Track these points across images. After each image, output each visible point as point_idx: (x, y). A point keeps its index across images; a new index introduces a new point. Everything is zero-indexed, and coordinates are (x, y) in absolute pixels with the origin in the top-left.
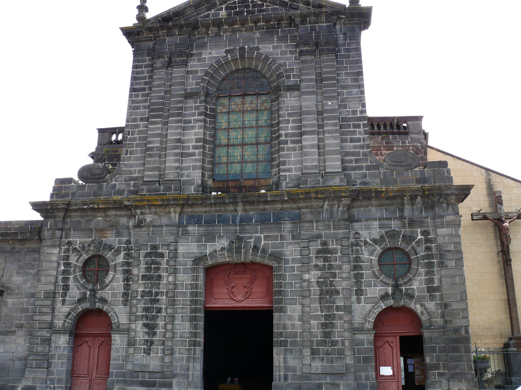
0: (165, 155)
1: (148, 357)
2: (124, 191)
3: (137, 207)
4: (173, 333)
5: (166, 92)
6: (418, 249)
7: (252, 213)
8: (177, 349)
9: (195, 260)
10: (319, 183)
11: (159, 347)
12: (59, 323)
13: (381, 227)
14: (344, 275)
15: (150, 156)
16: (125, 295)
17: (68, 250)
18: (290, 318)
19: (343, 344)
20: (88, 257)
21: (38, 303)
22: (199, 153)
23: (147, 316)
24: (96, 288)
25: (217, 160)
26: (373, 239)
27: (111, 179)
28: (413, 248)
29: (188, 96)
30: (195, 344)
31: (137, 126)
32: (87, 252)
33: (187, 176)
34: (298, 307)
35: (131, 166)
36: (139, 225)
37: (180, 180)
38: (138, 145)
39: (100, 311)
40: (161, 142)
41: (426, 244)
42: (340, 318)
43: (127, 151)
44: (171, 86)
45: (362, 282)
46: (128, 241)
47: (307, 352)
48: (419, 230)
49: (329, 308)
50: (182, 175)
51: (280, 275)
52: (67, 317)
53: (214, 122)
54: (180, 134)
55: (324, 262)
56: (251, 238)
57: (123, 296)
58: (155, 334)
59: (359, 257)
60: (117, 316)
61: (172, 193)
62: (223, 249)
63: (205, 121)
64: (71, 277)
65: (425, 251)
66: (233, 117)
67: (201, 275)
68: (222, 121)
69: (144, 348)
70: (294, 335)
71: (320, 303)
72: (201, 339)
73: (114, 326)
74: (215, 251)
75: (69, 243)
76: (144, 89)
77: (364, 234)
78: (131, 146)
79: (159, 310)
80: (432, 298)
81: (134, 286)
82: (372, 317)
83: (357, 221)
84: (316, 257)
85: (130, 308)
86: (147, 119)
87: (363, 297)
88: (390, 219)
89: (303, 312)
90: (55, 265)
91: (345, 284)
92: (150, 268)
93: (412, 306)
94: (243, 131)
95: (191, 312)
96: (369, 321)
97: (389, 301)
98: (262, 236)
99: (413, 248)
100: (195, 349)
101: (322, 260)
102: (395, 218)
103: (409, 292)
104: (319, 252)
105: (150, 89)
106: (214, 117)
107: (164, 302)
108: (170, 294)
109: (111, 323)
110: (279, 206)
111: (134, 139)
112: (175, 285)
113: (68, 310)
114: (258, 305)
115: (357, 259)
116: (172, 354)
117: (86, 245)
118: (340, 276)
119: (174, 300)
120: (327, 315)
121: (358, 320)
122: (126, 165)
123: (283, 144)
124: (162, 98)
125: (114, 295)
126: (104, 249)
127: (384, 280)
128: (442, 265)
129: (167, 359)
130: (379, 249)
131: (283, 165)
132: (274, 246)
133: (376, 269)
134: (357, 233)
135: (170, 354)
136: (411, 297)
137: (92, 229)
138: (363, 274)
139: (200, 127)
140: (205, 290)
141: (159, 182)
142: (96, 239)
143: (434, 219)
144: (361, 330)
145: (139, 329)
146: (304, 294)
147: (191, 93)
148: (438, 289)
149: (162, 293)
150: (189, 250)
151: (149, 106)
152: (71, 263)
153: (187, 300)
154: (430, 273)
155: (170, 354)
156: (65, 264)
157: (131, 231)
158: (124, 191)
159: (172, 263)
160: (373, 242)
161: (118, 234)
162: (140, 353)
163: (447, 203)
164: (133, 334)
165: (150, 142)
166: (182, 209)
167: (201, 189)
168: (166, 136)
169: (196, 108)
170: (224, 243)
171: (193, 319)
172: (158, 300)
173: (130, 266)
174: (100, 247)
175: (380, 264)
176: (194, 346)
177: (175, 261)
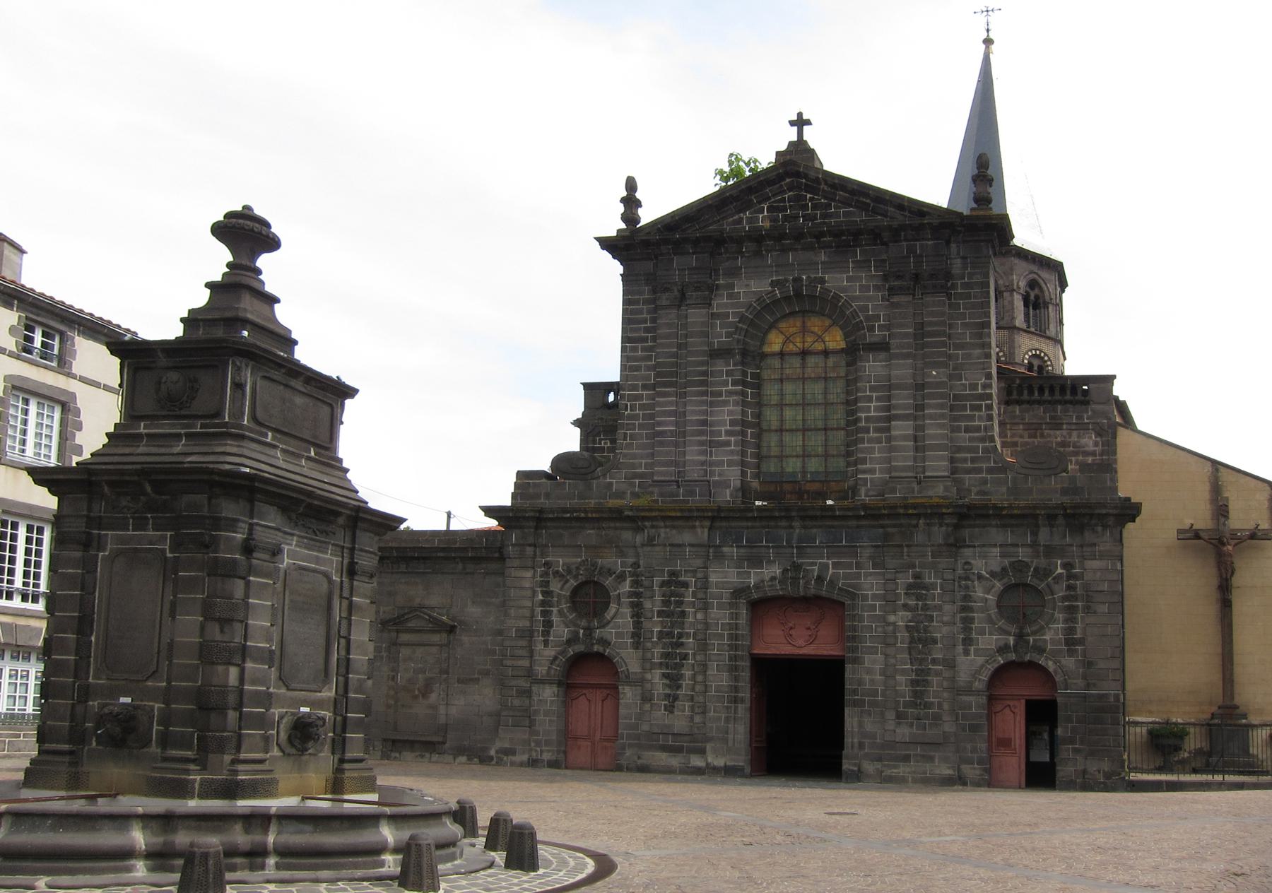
0: (685, 442)
1: (670, 716)
2: (624, 493)
3: (644, 518)
4: (706, 685)
5: (680, 346)
6: (1056, 587)
7: (814, 531)
8: (711, 706)
9: (734, 592)
10: (913, 492)
11: (686, 704)
12: (541, 670)
13: (1003, 555)
14: (945, 619)
15: (662, 444)
16: (636, 635)
17: (545, 574)
18: (869, 671)
19: (940, 705)
20: (578, 582)
21: (507, 643)
22: (735, 441)
23: (667, 663)
24: (592, 625)
25: (764, 451)
26: (991, 571)
27: (604, 476)
28: (1048, 585)
29: (716, 354)
30: (736, 700)
31: (640, 397)
32: (576, 577)
33: (720, 475)
34: (880, 657)
35: (634, 456)
36: (650, 542)
37: (709, 481)
38: (641, 426)
39: (600, 656)
40: (677, 424)
41: (1068, 580)
42: (938, 673)
43: (625, 434)
44: (686, 336)
45: (971, 629)
46: (635, 563)
47: (891, 715)
48: (1059, 562)
49: (921, 661)
50: (712, 473)
51: (854, 616)
52: (552, 662)
53: (759, 395)
54: (705, 413)
55: (917, 600)
56: (815, 564)
57: (632, 637)
58: (679, 687)
59: (970, 596)
60: (625, 662)
61: (697, 500)
62: (773, 579)
63: (743, 394)
64: (555, 610)
65: (1066, 590)
66: (789, 388)
67: (744, 611)
68: (771, 391)
69: (665, 705)
70: (875, 693)
71: (910, 654)
72: (746, 694)
73: (622, 676)
74: (763, 581)
75: (547, 564)
76: (645, 340)
77: (979, 566)
78: (631, 427)
79: (685, 657)
80: (1071, 653)
81: (646, 625)
82: (984, 675)
83: (969, 546)
84: (905, 594)
85: (643, 653)
86: (654, 387)
87: (972, 648)
88: (1017, 546)
89: (886, 665)
90: (529, 593)
91: (945, 630)
92: (670, 601)
93: (1042, 662)
94: (803, 409)
95: (730, 659)
96: (980, 679)
97: (1010, 654)
98: (830, 562)
99: (1048, 585)
100: (736, 708)
101: (914, 598)
102: (1023, 546)
103: (1038, 644)
104: (910, 587)
105: (654, 339)
106: (758, 386)
107: (691, 645)
108: (700, 636)
109: (617, 672)
110: (853, 523)
111: (635, 417)
112: (707, 626)
113: (553, 653)
114: (825, 653)
115: (967, 598)
116: (704, 713)
117: (573, 567)
118: (939, 619)
119: (707, 644)
120: (920, 669)
121: (963, 676)
122: (625, 456)
123: (861, 433)
124: (676, 355)
125: (619, 635)
126: (600, 573)
127: (1004, 627)
128: (1088, 610)
129: (698, 719)
130: (999, 586)
131: (862, 464)
132: (846, 576)
133: (994, 611)
134: (967, 563)
135: (702, 713)
136: (1041, 650)
137: (580, 546)
138: (973, 618)
139: (736, 403)
140: (751, 631)
141: (677, 482)
142: (587, 560)
143: (1082, 546)
144: (969, 691)
145: (657, 680)
146: (888, 641)
147: (719, 350)
148: (1081, 641)
149: (688, 635)
150: (726, 578)
151: (654, 368)
152: (552, 592)
153: (724, 644)
154: (1071, 620)
155: (702, 713)
156: (544, 593)
157: (640, 550)
158: (624, 493)
159: (700, 595)
160: (991, 576)
161: (622, 554)
162: (660, 710)
163: (1102, 526)
164: (648, 686)
165: (659, 424)
166: (712, 522)
167: (740, 494)
168: (684, 413)
169: (729, 373)
170: (777, 570)
171: (733, 669)
172: (682, 644)
173: (641, 597)
174: (594, 571)
175: (999, 606)
176: (735, 702)
177: (706, 593)
